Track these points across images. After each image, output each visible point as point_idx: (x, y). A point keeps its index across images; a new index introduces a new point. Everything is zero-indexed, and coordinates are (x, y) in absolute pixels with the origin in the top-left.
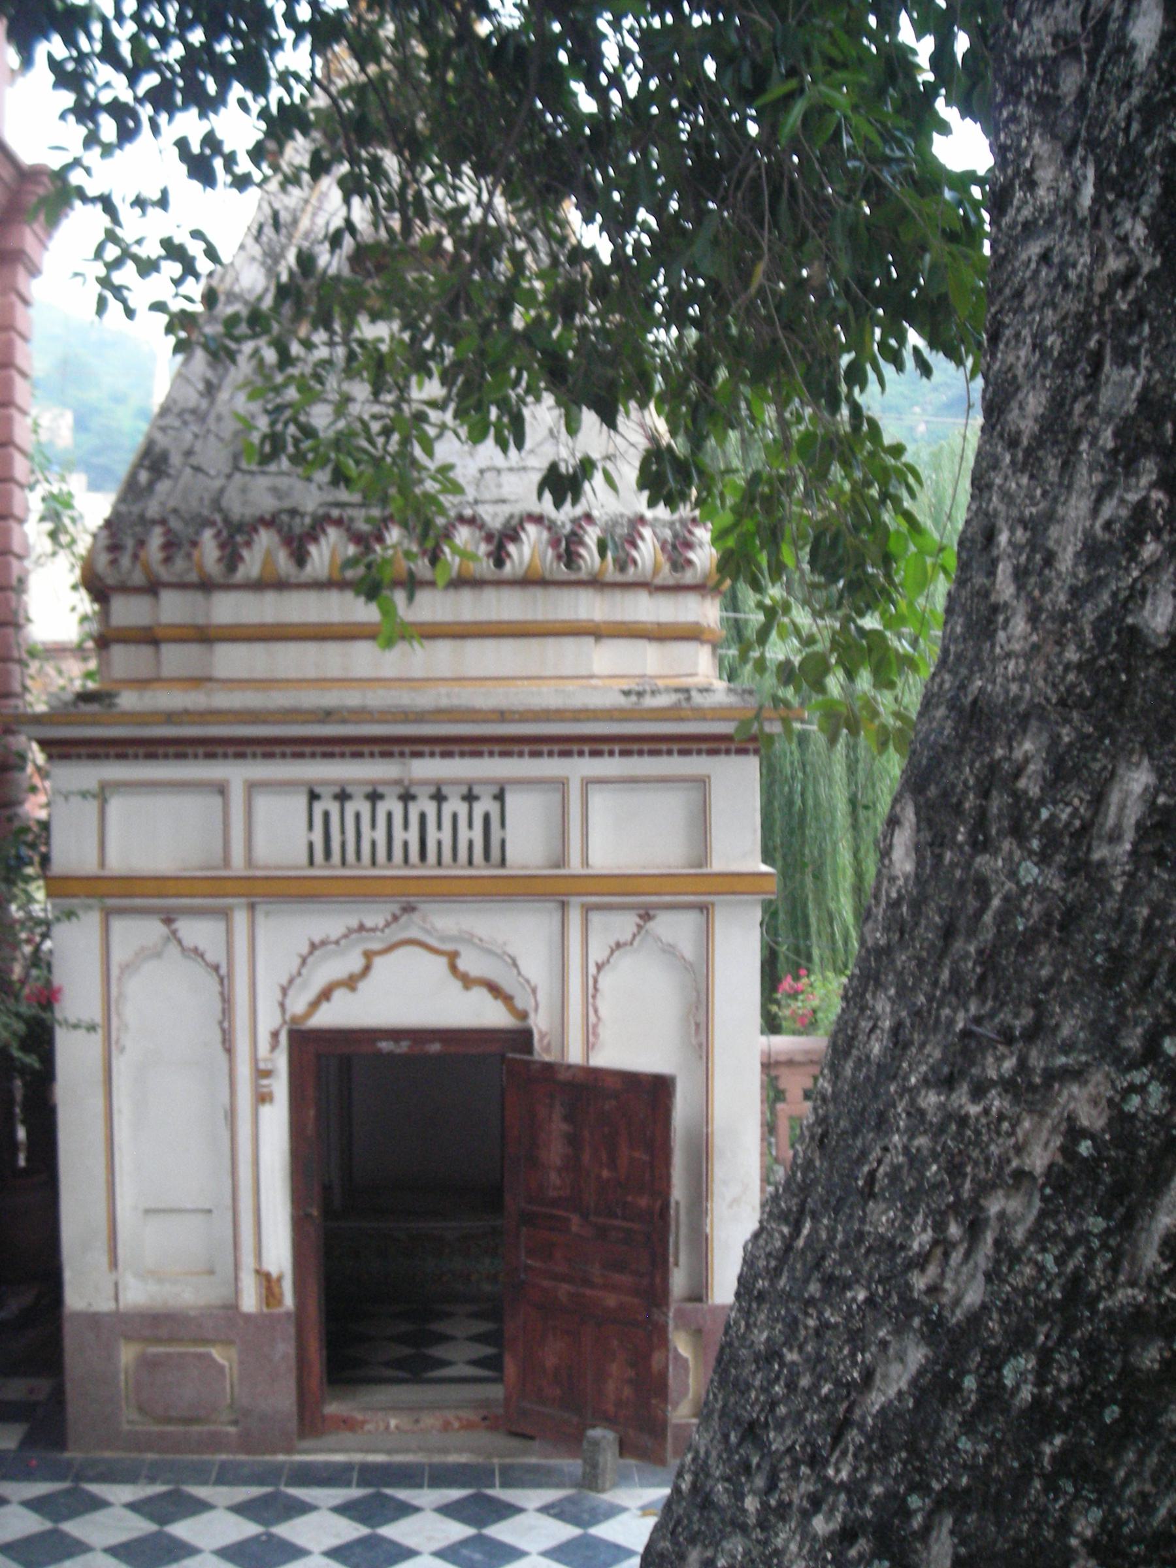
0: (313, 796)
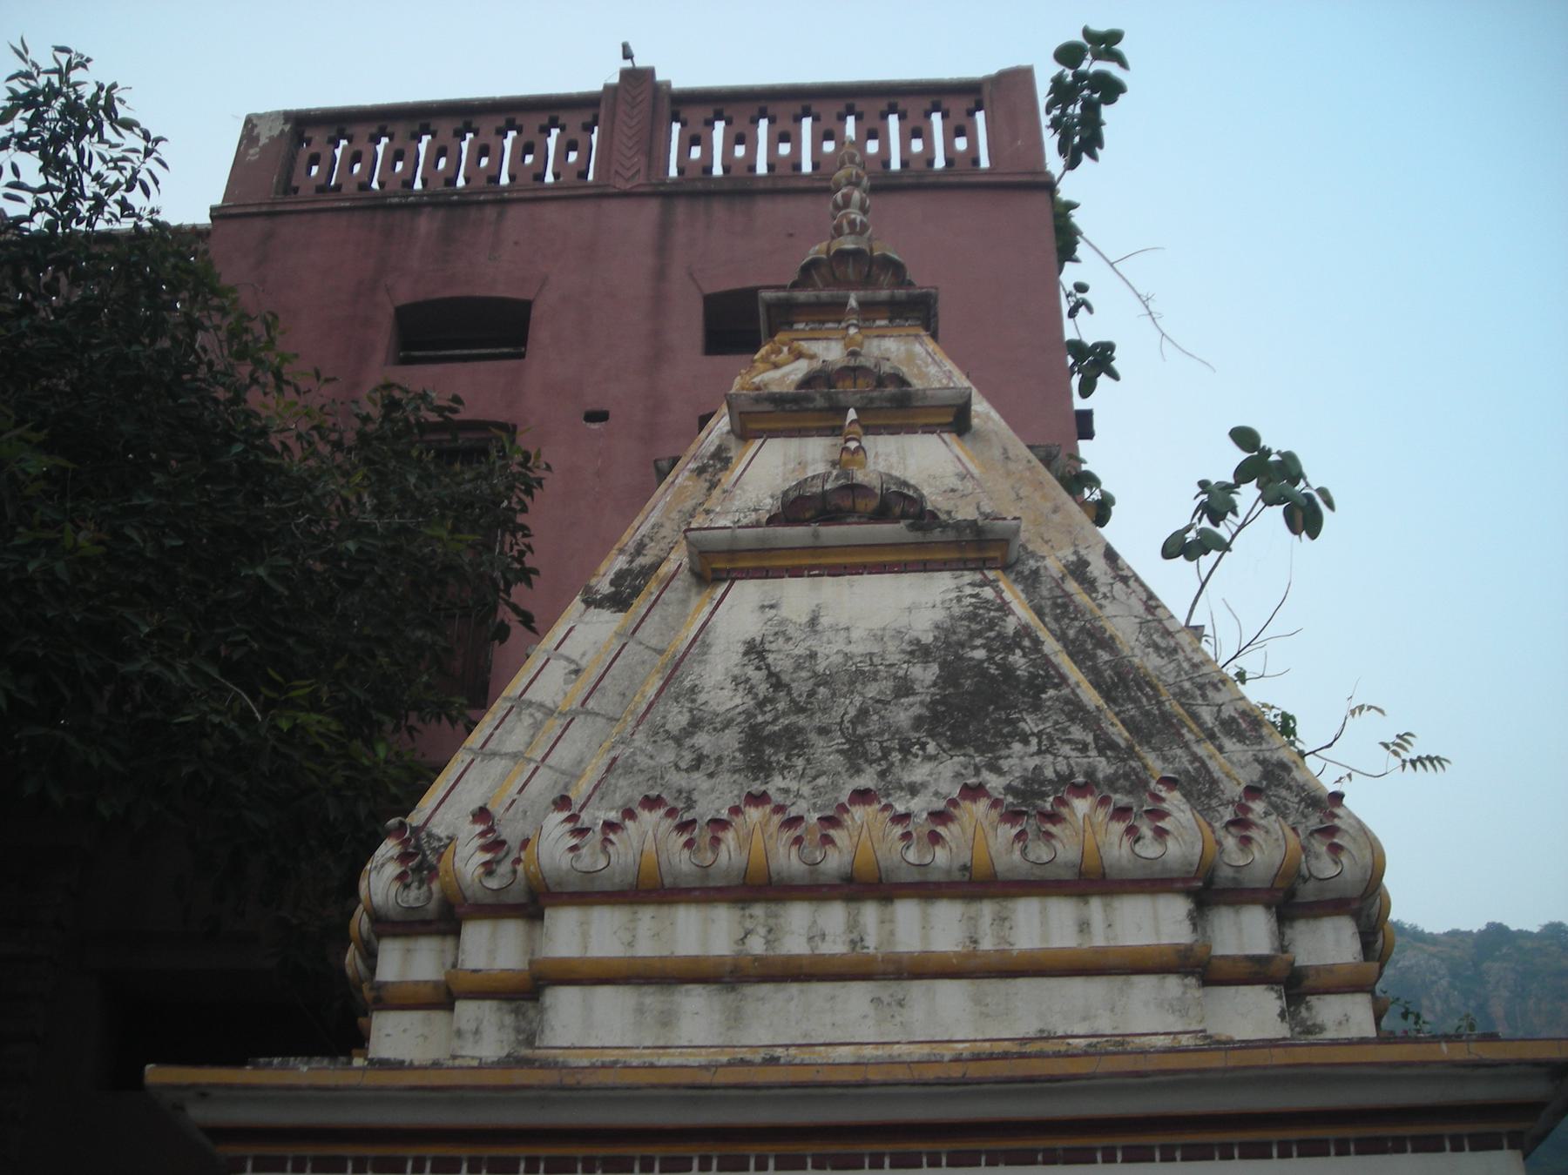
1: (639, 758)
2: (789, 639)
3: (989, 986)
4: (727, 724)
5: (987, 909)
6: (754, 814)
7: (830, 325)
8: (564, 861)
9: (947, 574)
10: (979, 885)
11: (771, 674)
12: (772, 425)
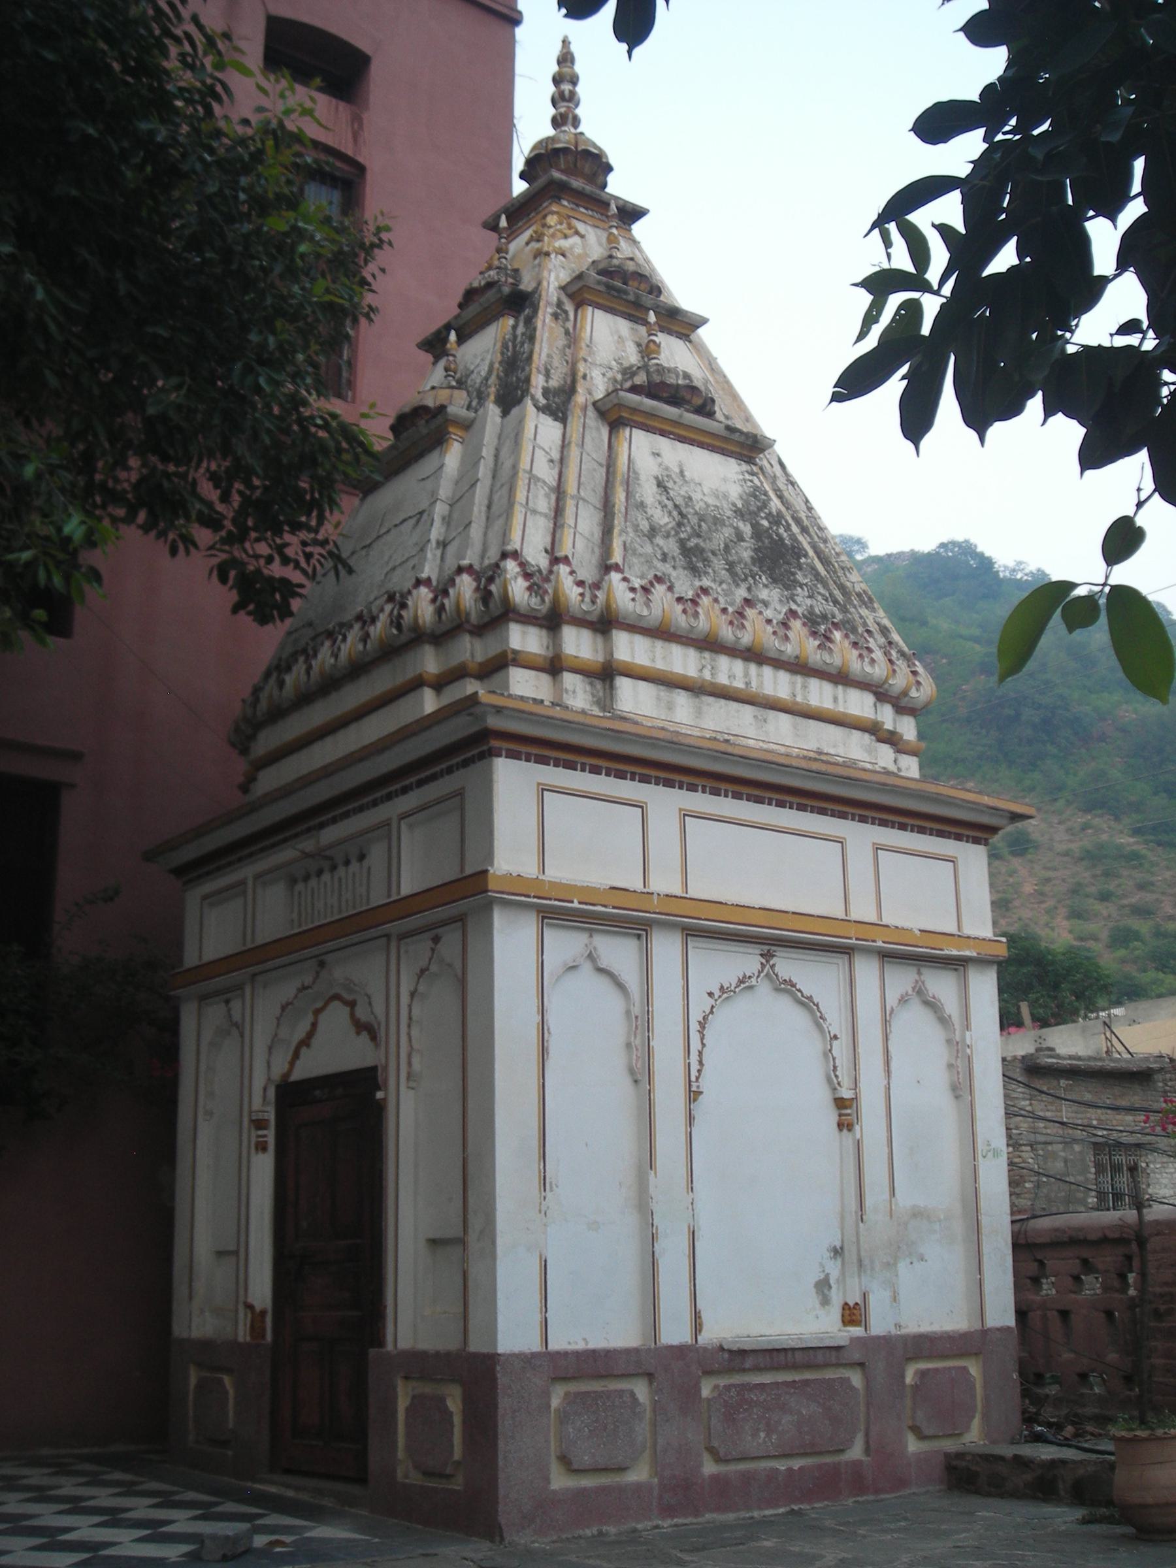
0: (293, 881)
1: (637, 546)
2: (675, 482)
3: (799, 720)
4: (667, 536)
5: (799, 679)
6: (705, 600)
7: (582, 210)
8: (631, 606)
9: (733, 460)
10: (799, 667)
11: (676, 506)
12: (600, 301)
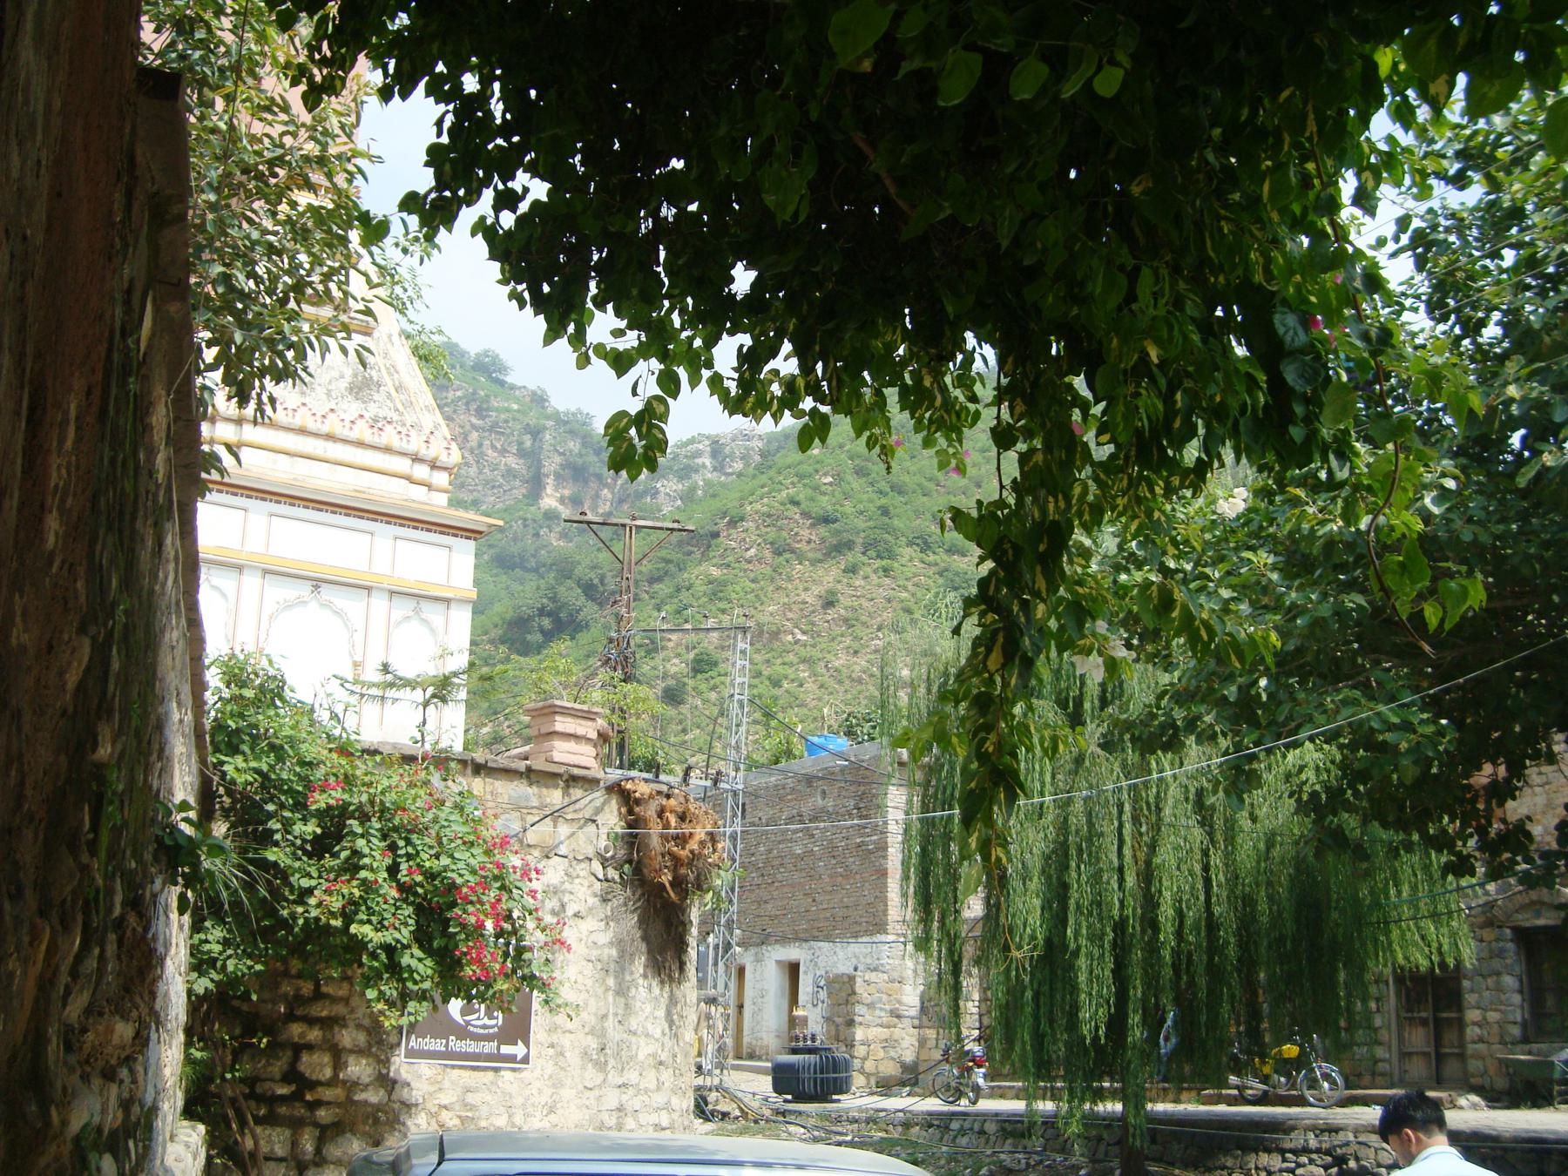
10: (360, 444)
